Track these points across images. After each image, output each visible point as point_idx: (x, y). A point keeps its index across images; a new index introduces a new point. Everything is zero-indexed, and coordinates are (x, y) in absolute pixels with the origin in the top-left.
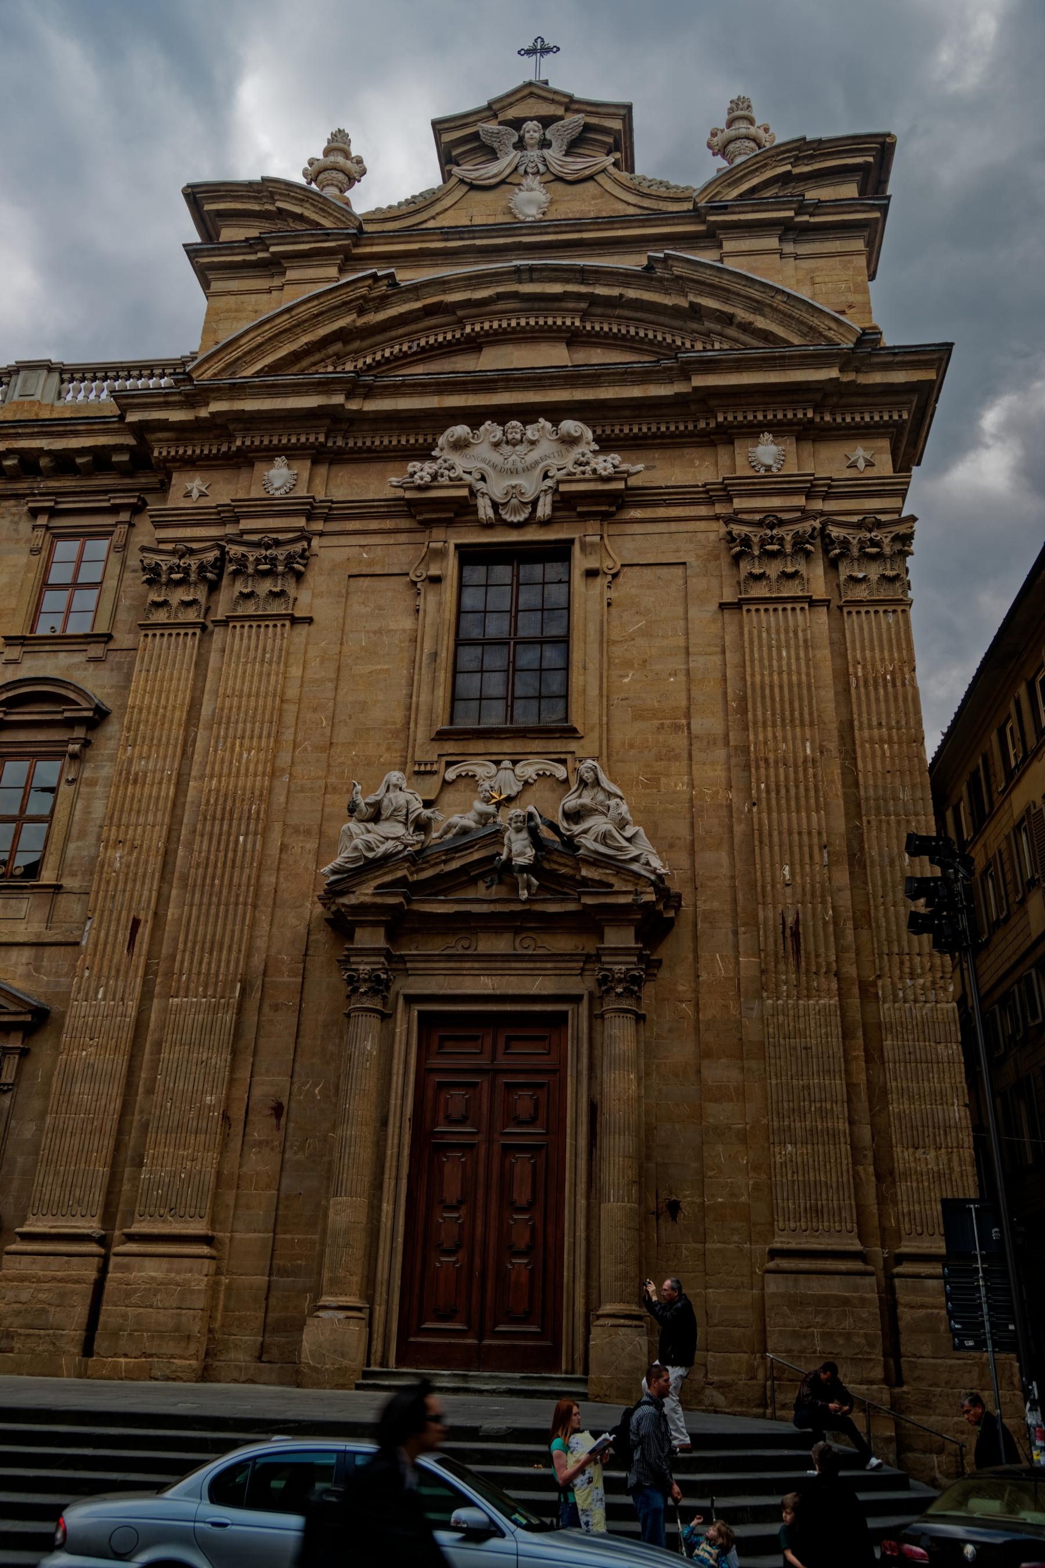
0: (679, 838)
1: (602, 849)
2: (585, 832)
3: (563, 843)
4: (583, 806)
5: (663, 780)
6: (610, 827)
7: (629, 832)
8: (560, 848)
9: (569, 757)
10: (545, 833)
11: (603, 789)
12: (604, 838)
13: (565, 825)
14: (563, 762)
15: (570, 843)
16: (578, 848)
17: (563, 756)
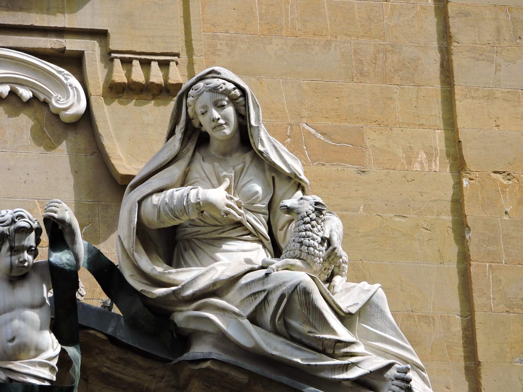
0: (426, 319)
1: (277, 347)
2: (217, 290)
3: (132, 322)
4: (203, 207)
5: (373, 138)
6: (302, 277)
7: (349, 294)
8: (123, 335)
9: (91, 49)
10: (90, 292)
11: (261, 160)
12: (291, 314)
13: (145, 263)
14: (74, 62)
15: (156, 327)
16: (184, 339)
17: (72, 44)
